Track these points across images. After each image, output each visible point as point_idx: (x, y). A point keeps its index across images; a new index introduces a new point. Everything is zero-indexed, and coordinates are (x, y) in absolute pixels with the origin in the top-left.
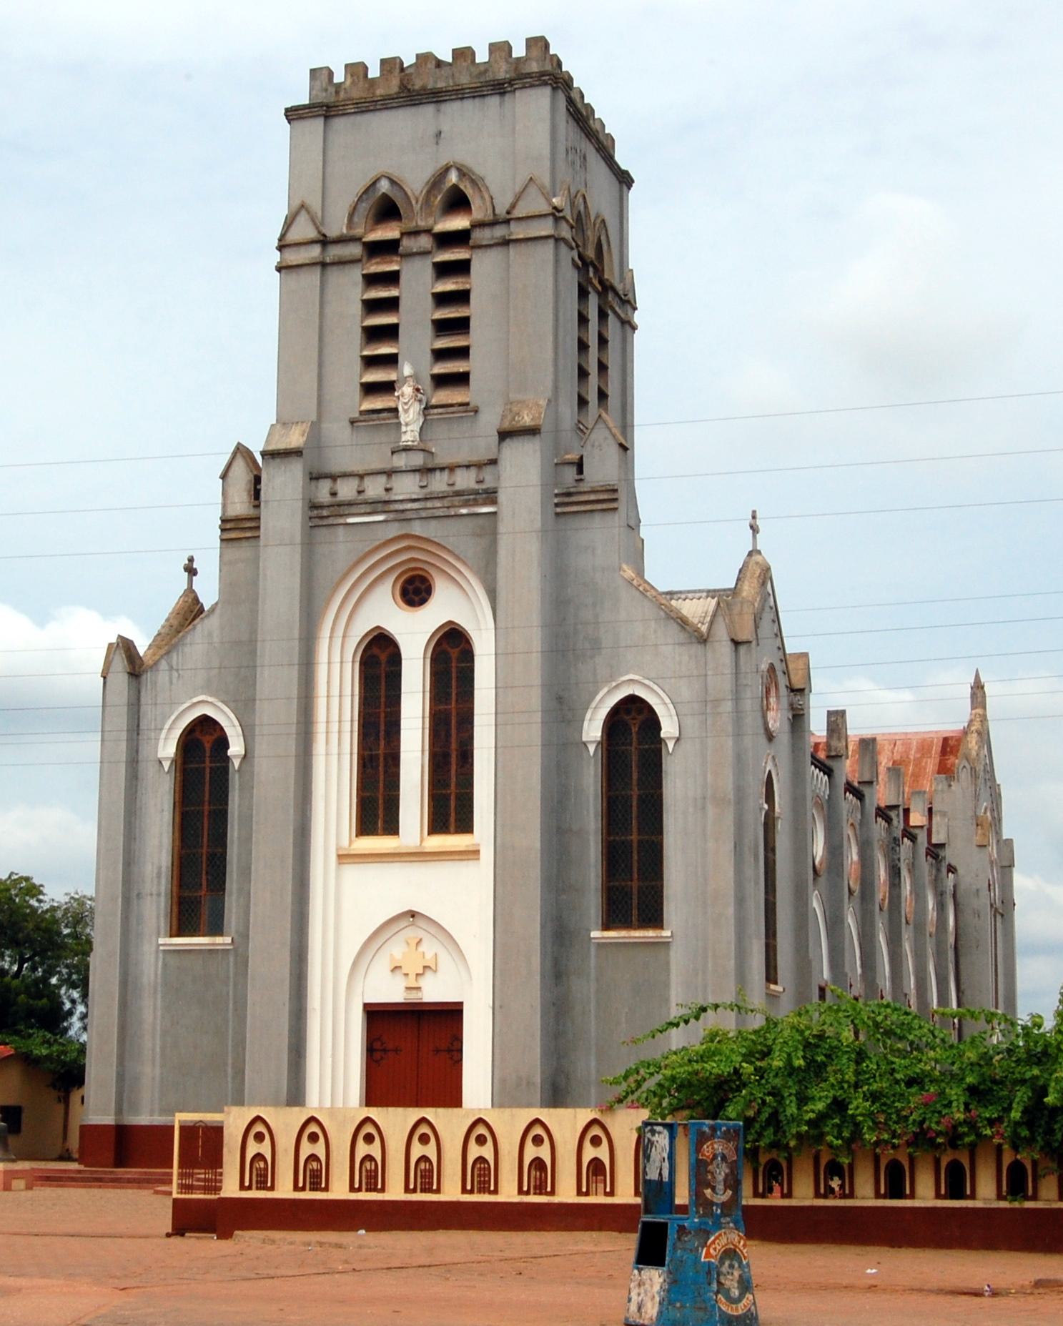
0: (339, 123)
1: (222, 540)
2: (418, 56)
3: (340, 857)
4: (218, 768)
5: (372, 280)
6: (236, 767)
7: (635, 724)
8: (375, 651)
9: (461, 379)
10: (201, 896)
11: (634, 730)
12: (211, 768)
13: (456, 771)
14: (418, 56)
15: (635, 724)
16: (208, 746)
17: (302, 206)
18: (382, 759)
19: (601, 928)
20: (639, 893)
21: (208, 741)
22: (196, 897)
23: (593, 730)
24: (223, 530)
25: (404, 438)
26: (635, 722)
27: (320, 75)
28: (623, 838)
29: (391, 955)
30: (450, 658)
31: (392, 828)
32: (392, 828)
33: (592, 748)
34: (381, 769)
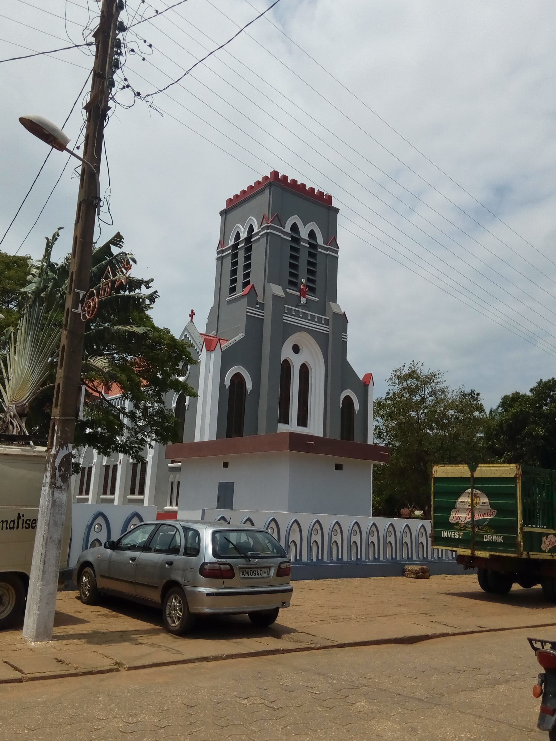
2: (302, 183)
25: (302, 302)
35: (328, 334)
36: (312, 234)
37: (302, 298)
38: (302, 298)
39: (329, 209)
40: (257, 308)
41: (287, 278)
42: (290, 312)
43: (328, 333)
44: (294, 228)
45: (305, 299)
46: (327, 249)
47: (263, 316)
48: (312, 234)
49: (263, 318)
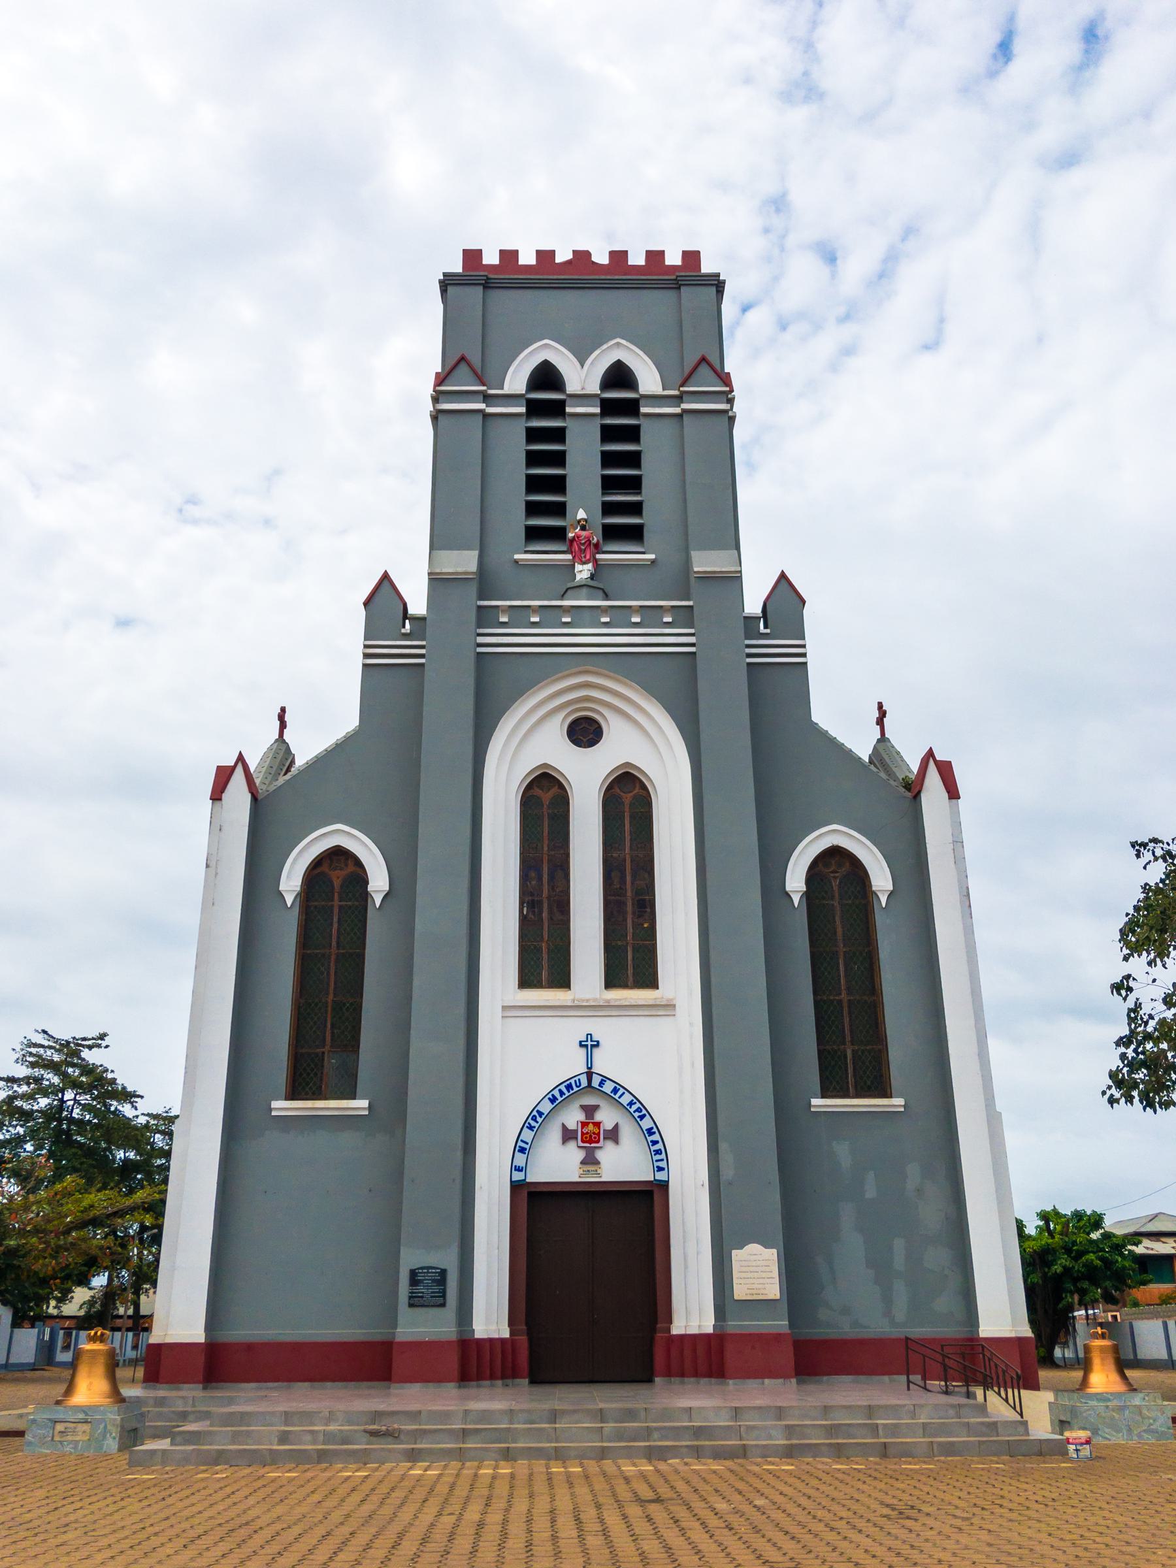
0: (497, 296)
1: (365, 665)
2: (574, 251)
3: (504, 1008)
4: (350, 907)
5: (533, 435)
6: (377, 907)
7: (835, 878)
8: (537, 791)
9: (635, 534)
10: (323, 1053)
11: (835, 884)
12: (340, 907)
13: (633, 922)
14: (574, 251)
15: (835, 878)
16: (337, 883)
17: (463, 359)
18: (545, 905)
19: (820, 1095)
20: (853, 1057)
21: (337, 877)
22: (317, 1055)
23: (796, 881)
24: (366, 656)
25: (578, 577)
26: (837, 875)
27: (472, 257)
28: (832, 998)
29: (563, 1125)
30: (634, 797)
31: (562, 980)
32: (562, 980)
33: (796, 899)
34: (545, 915)
35: (694, 653)
36: (619, 376)
37: (578, 567)
38: (578, 567)
39: (679, 288)
40: (406, 636)
41: (518, 520)
42: (519, 615)
43: (692, 649)
44: (546, 377)
45: (590, 566)
46: (680, 399)
47: (422, 656)
48: (619, 376)
49: (422, 661)
